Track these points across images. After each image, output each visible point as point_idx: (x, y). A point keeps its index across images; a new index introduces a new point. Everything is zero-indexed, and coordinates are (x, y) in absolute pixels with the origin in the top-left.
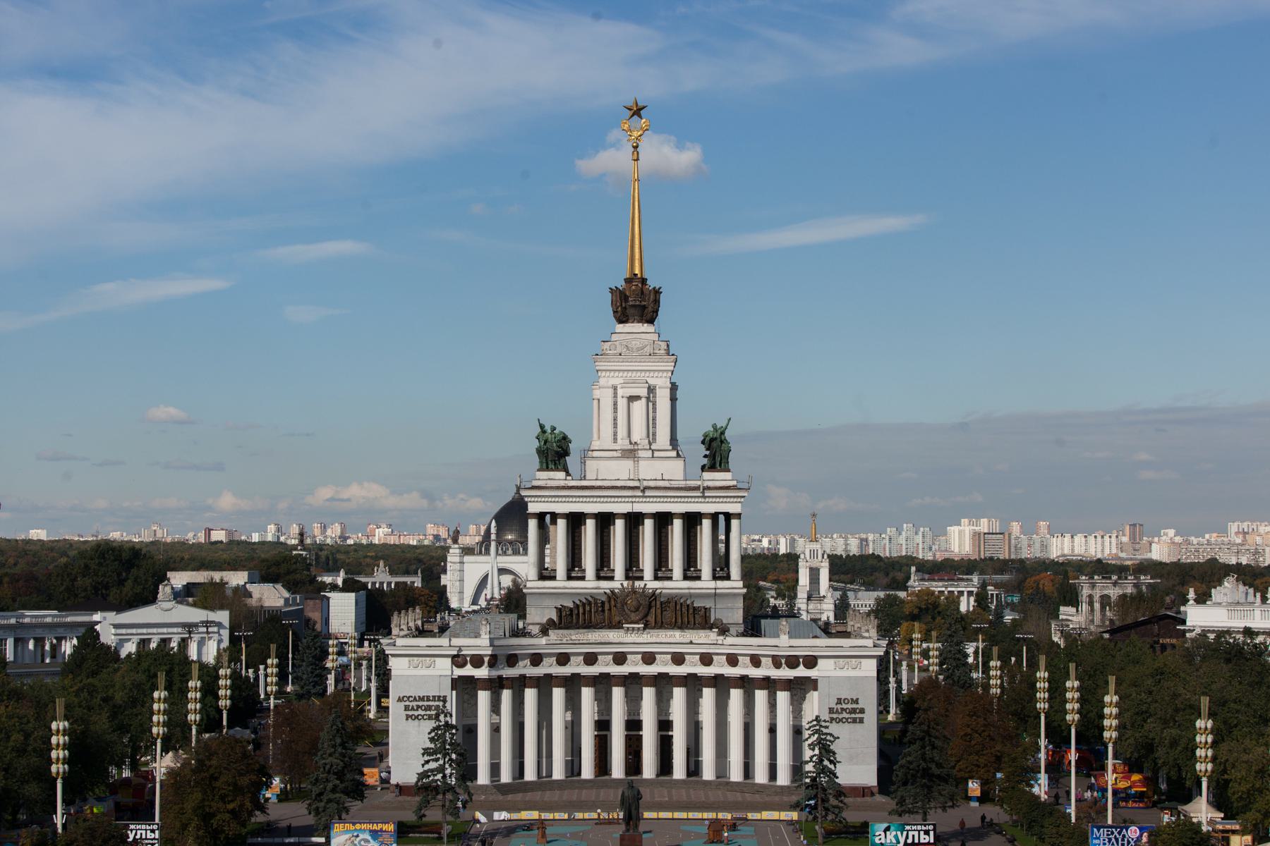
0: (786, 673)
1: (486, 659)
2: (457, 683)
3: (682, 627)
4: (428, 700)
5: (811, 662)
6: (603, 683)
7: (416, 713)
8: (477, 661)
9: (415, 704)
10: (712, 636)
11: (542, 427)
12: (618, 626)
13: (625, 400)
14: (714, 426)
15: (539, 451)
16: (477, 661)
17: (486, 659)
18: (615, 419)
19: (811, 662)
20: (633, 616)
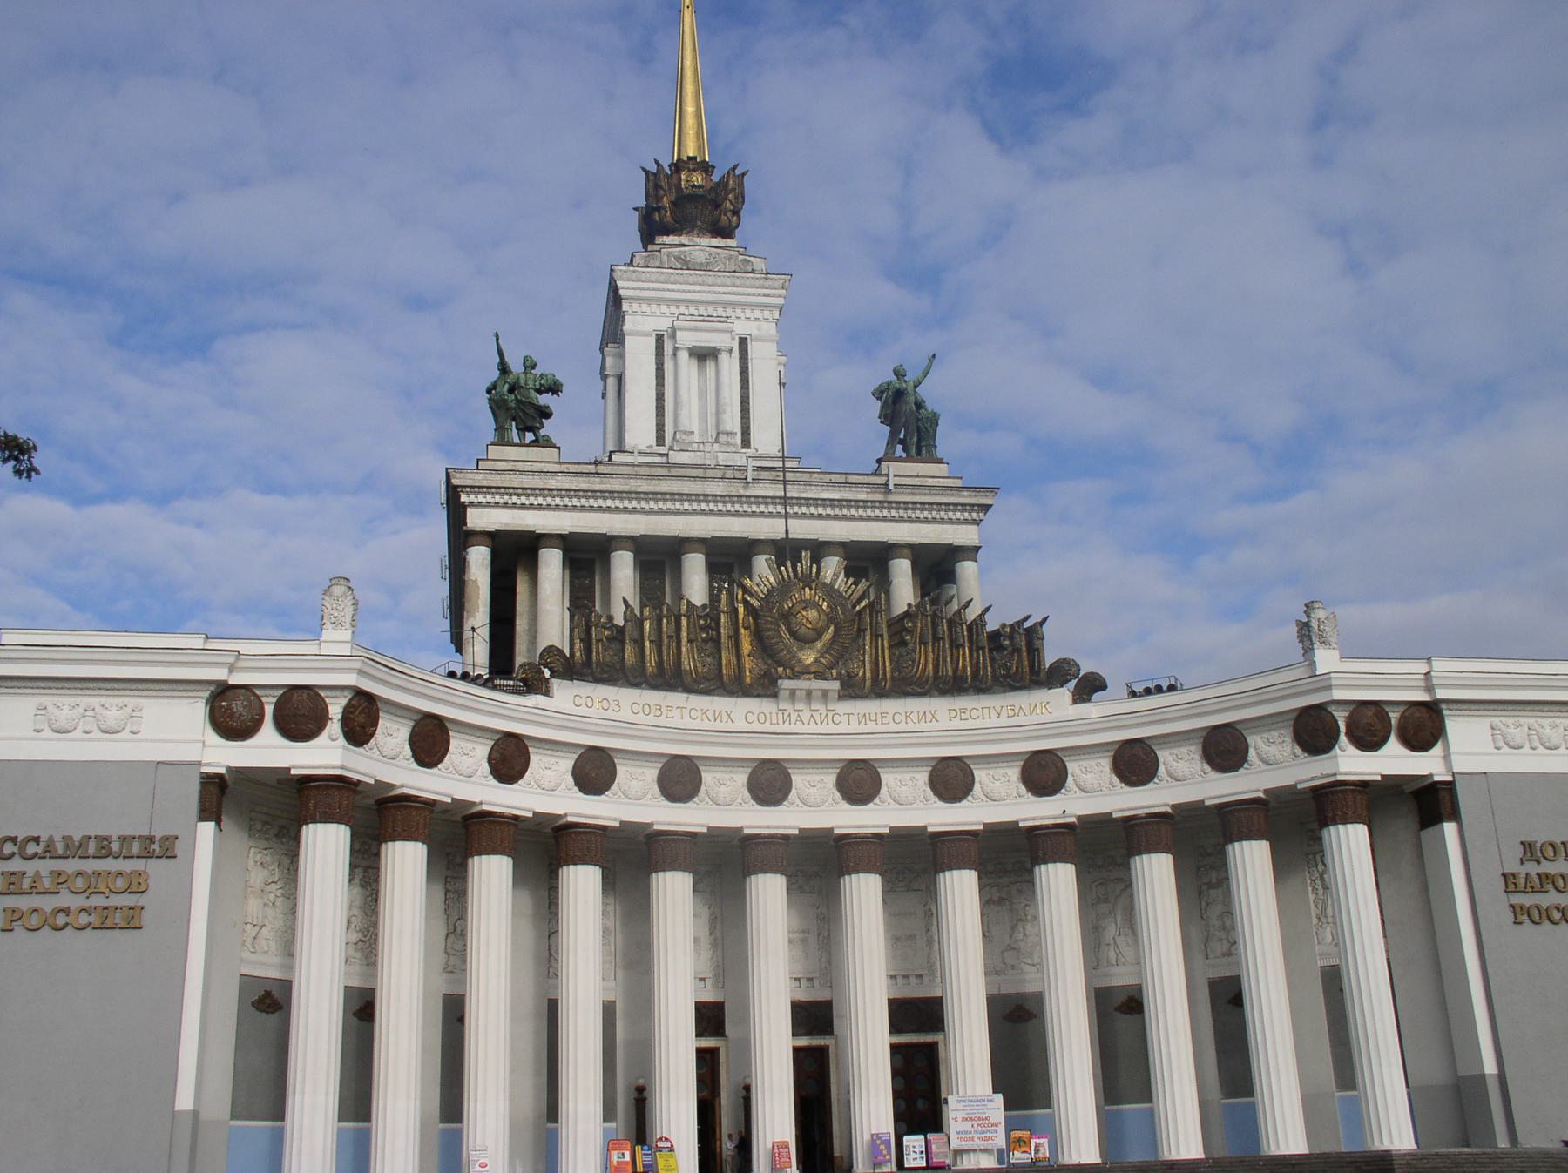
0: (1352, 763)
1: (336, 709)
2: (218, 795)
3: (954, 686)
4: (104, 851)
5: (1423, 725)
6: (724, 863)
7: (48, 903)
8: (300, 714)
9: (45, 866)
10: (1057, 703)
11: (504, 369)
12: (766, 687)
13: (683, 356)
14: (898, 373)
15: (498, 406)
16: (300, 714)
17: (336, 709)
18: (660, 398)
19: (1423, 725)
20: (809, 657)
